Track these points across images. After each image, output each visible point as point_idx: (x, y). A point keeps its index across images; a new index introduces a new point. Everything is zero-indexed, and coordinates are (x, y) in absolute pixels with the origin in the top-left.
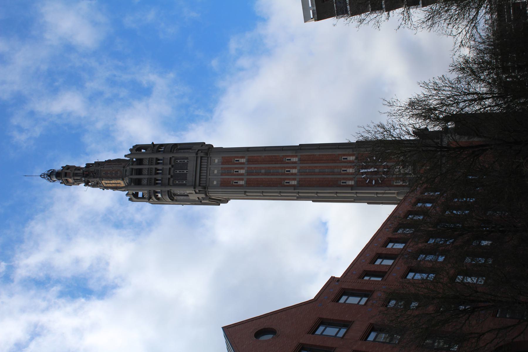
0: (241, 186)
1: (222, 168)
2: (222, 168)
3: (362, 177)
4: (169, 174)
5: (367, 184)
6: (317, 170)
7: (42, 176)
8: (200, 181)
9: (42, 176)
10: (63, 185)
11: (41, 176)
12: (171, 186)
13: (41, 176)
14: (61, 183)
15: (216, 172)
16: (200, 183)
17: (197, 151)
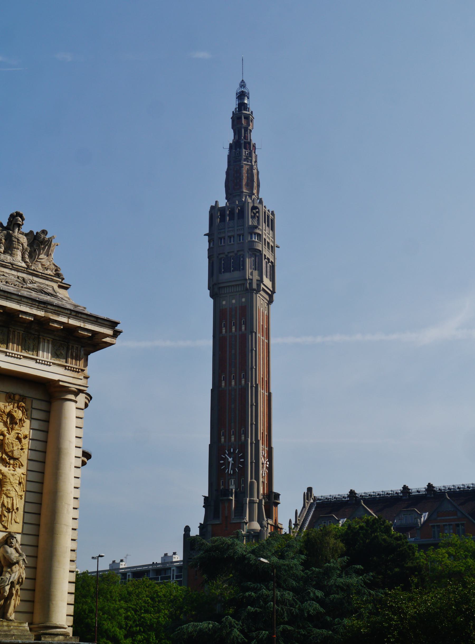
0: (221, 332)
1: (236, 308)
2: (236, 308)
3: (226, 451)
4: (228, 253)
5: (221, 456)
6: (233, 406)
7: (243, 84)
8: (224, 287)
9: (243, 84)
10: (231, 116)
11: (243, 80)
12: (218, 257)
13: (243, 80)
14: (233, 112)
15: (234, 301)
16: (222, 287)
17: (251, 277)
